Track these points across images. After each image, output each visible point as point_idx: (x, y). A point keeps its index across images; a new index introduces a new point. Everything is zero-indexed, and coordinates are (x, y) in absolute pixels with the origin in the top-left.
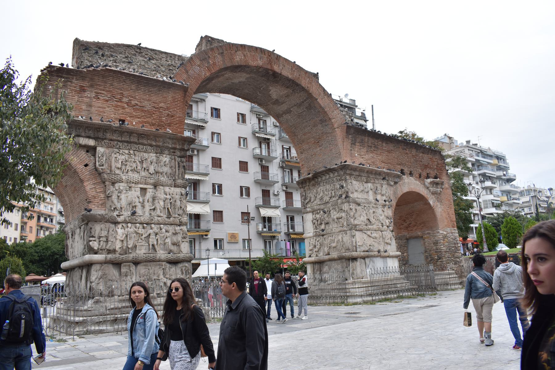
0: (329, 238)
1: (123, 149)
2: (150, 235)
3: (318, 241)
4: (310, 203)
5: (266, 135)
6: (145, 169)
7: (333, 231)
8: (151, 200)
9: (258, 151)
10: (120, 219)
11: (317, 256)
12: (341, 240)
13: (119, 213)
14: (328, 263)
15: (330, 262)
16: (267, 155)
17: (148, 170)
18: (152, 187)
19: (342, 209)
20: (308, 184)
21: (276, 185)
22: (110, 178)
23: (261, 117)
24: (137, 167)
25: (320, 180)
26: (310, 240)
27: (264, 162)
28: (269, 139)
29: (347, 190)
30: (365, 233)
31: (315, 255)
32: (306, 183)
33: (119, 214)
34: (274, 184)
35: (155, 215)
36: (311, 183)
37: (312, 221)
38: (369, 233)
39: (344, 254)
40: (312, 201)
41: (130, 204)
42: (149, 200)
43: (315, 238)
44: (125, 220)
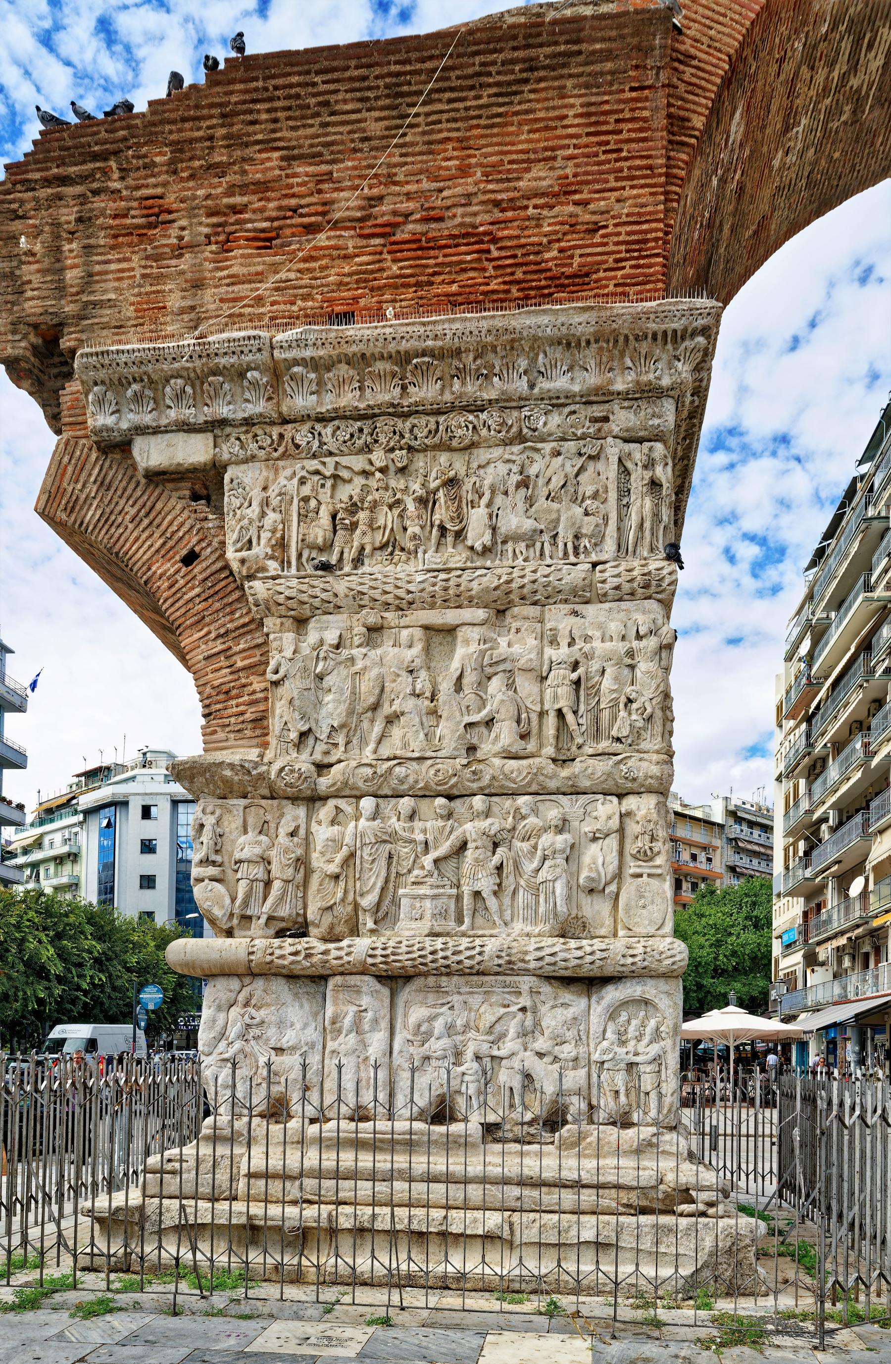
1: (342, 454)
2: (463, 846)
6: (443, 529)
8: (470, 679)
10: (324, 783)
13: (327, 753)
17: (459, 535)
18: (481, 614)
22: (281, 599)
24: (405, 529)
33: (327, 760)
35: (497, 748)
41: (375, 707)
42: (466, 681)
44: (346, 784)
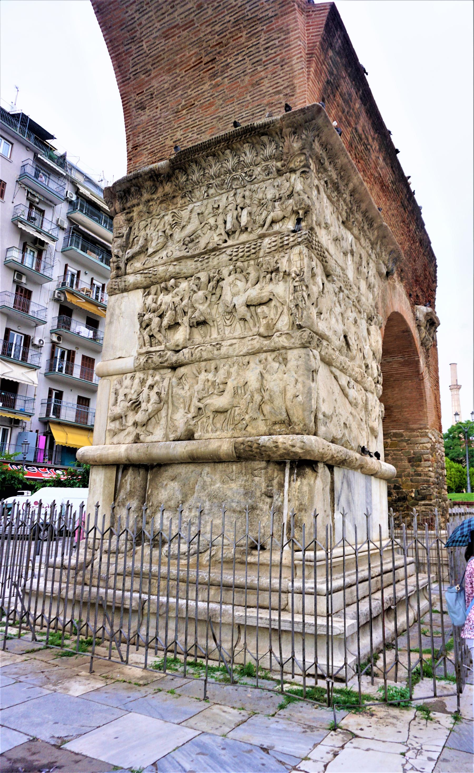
0: (203, 376)
3: (151, 387)
4: (143, 258)
5: (40, 233)
7: (224, 350)
9: (16, 255)
11: (137, 440)
12: (254, 384)
14: (183, 470)
15: (191, 467)
16: (34, 268)
19: (277, 270)
20: (146, 196)
21: (41, 327)
23: (37, 200)
25: (195, 177)
26: (120, 383)
27: (24, 280)
28: (43, 243)
29: (308, 202)
30: (336, 378)
31: (131, 438)
32: (139, 188)
34: (37, 325)
36: (159, 194)
37: (141, 316)
38: (344, 380)
39: (264, 440)
40: (150, 251)
43: (139, 375)
